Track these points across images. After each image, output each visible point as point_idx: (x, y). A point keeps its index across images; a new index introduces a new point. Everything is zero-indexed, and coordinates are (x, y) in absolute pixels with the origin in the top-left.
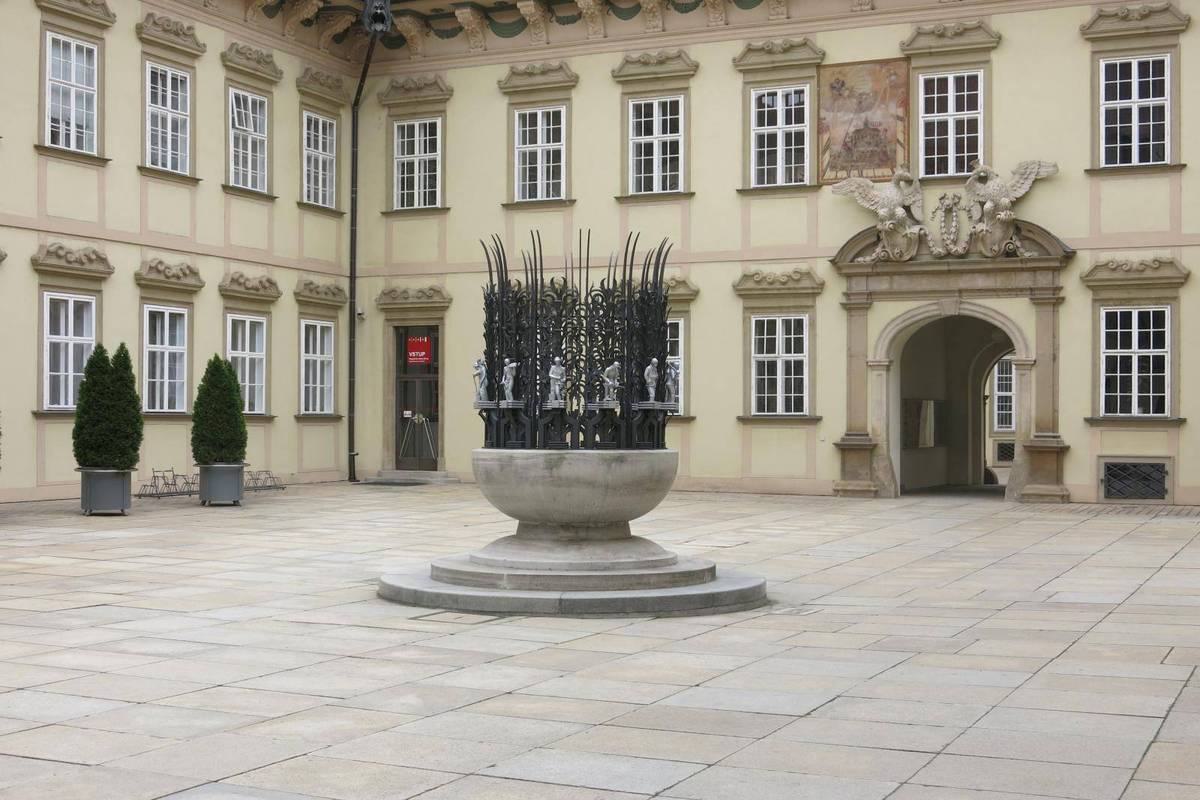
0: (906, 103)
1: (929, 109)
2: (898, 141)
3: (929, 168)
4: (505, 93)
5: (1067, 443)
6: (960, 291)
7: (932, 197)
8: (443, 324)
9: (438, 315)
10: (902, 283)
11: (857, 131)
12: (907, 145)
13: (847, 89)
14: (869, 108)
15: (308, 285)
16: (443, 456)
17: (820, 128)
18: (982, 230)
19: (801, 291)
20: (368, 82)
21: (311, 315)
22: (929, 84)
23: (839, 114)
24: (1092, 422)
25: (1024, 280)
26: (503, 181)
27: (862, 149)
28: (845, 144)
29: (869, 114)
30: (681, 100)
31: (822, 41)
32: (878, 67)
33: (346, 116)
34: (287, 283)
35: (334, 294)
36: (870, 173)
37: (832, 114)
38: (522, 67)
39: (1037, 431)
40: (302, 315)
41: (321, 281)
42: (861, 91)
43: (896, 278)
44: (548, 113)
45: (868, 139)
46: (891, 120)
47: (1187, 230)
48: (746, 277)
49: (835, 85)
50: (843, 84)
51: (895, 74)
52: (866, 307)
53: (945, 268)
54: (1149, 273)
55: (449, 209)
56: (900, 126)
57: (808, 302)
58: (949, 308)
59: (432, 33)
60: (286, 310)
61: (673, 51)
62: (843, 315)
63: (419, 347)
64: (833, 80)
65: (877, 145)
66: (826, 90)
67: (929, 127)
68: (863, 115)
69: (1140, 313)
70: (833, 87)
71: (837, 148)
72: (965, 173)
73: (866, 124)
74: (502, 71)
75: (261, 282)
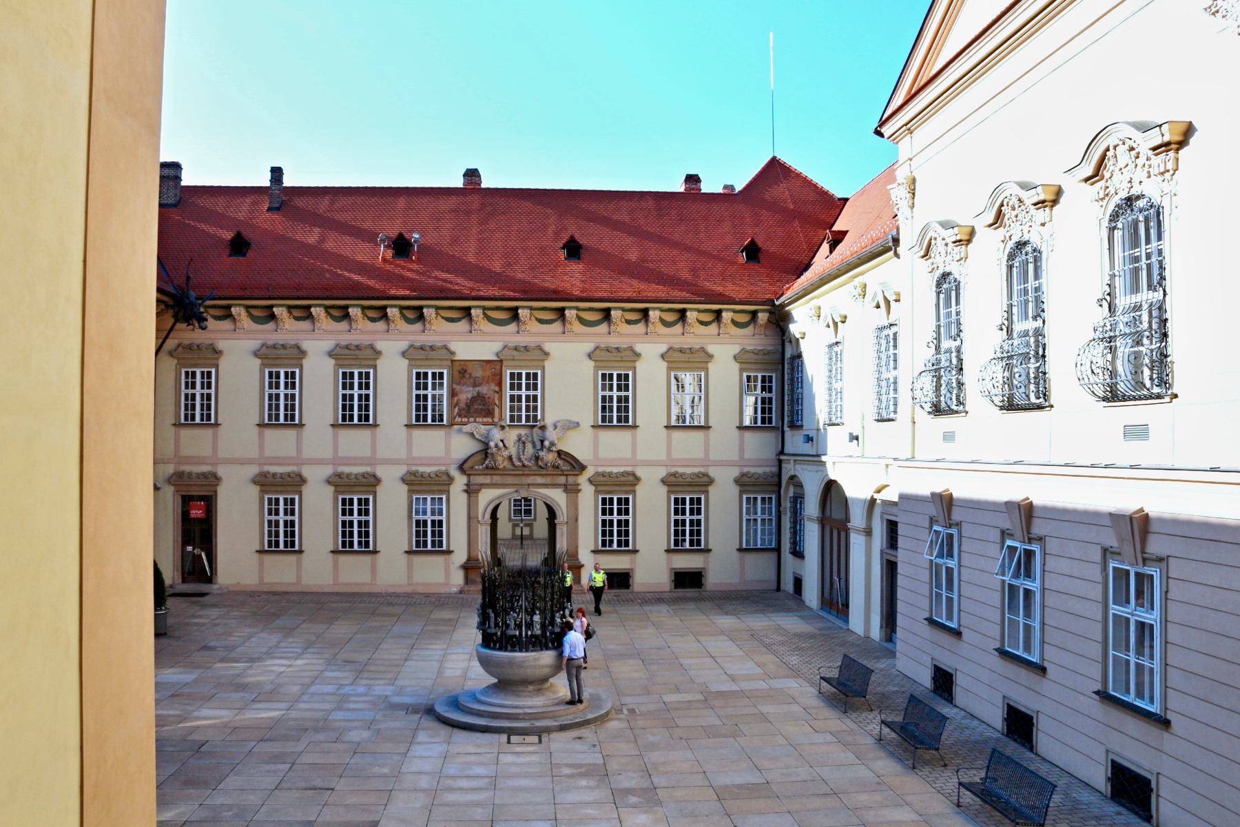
0: (500, 384)
1: (512, 388)
2: (496, 404)
5: (583, 563)
6: (529, 485)
7: (512, 436)
9: (213, 489)
10: (497, 479)
12: (500, 407)
14: (480, 385)
16: (216, 574)
17: (453, 394)
19: (440, 483)
22: (512, 375)
23: (463, 388)
24: (595, 552)
25: (562, 480)
27: (476, 407)
28: (466, 404)
31: (453, 346)
43: (494, 477)
46: (492, 392)
47: (639, 457)
50: (466, 371)
51: (494, 368)
52: (478, 491)
53: (521, 473)
54: (623, 479)
56: (497, 396)
57: (445, 488)
62: (465, 495)
64: (459, 368)
65: (484, 405)
66: (456, 373)
67: (512, 398)
68: (477, 389)
69: (618, 498)
70: (460, 372)
71: (462, 405)
73: (478, 393)
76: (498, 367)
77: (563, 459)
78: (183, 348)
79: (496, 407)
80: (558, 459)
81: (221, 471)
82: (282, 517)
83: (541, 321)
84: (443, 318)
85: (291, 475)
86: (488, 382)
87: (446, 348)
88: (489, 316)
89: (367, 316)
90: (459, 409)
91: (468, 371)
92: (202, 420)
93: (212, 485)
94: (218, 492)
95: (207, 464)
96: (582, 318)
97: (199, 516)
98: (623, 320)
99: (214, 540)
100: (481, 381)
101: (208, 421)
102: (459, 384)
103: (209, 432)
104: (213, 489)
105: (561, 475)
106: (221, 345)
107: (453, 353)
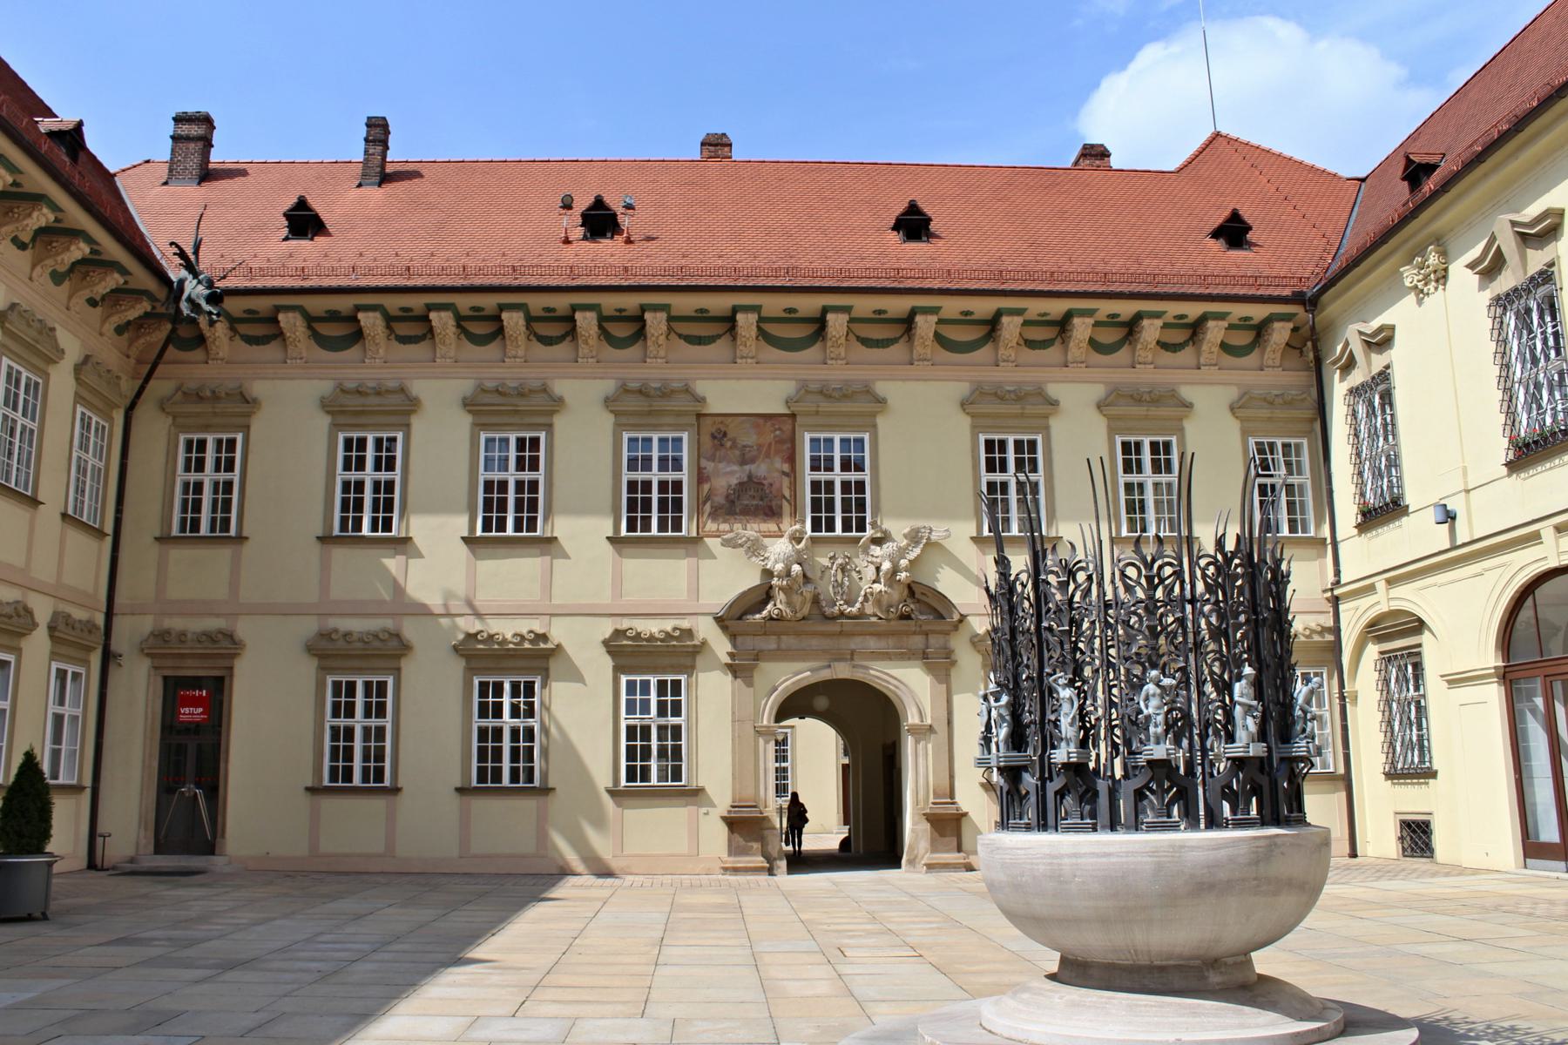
0: (792, 458)
2: (785, 497)
3: (816, 526)
4: (328, 412)
5: (965, 809)
8: (231, 676)
11: (741, 484)
13: (729, 440)
14: (753, 461)
15: (68, 620)
17: (701, 477)
18: (881, 591)
20: (152, 383)
21: (63, 655)
23: (721, 466)
25: (917, 641)
26: (319, 508)
27: (746, 502)
28: (727, 497)
29: (753, 467)
30: (542, 436)
31: (701, 387)
32: (761, 421)
33: (119, 417)
34: (43, 610)
35: (90, 632)
36: (755, 526)
37: (713, 464)
38: (351, 385)
39: (934, 798)
40: (54, 656)
41: (79, 614)
42: (745, 443)
43: (784, 638)
44: (351, 439)
45: (752, 493)
46: (776, 474)
48: (618, 633)
49: (716, 434)
50: (725, 434)
51: (780, 429)
55: (247, 538)
56: (786, 481)
58: (842, 671)
59: (237, 337)
60: (38, 644)
61: (536, 384)
63: (195, 702)
64: (714, 430)
65: (762, 499)
66: (706, 440)
67: (816, 486)
68: (747, 467)
70: (713, 437)
71: (720, 500)
72: (854, 534)
73: (750, 477)
74: (325, 387)
75: (16, 609)
76: (787, 427)
77: (919, 601)
78: (184, 393)
79: (785, 504)
80: (909, 601)
81: (244, 629)
82: (359, 722)
83: (866, 342)
84: (680, 336)
85: (381, 636)
86: (768, 455)
87: (687, 390)
88: (766, 332)
89: (536, 335)
90: (712, 507)
91: (731, 435)
92: (213, 529)
93: (221, 656)
94: (237, 671)
95: (218, 615)
96: (944, 337)
97: (198, 718)
98: (1022, 342)
99: (222, 765)
100: (755, 453)
101: (224, 534)
102: (712, 458)
103: (224, 553)
104: (226, 663)
105: (915, 633)
106: (258, 389)
107: (701, 400)
